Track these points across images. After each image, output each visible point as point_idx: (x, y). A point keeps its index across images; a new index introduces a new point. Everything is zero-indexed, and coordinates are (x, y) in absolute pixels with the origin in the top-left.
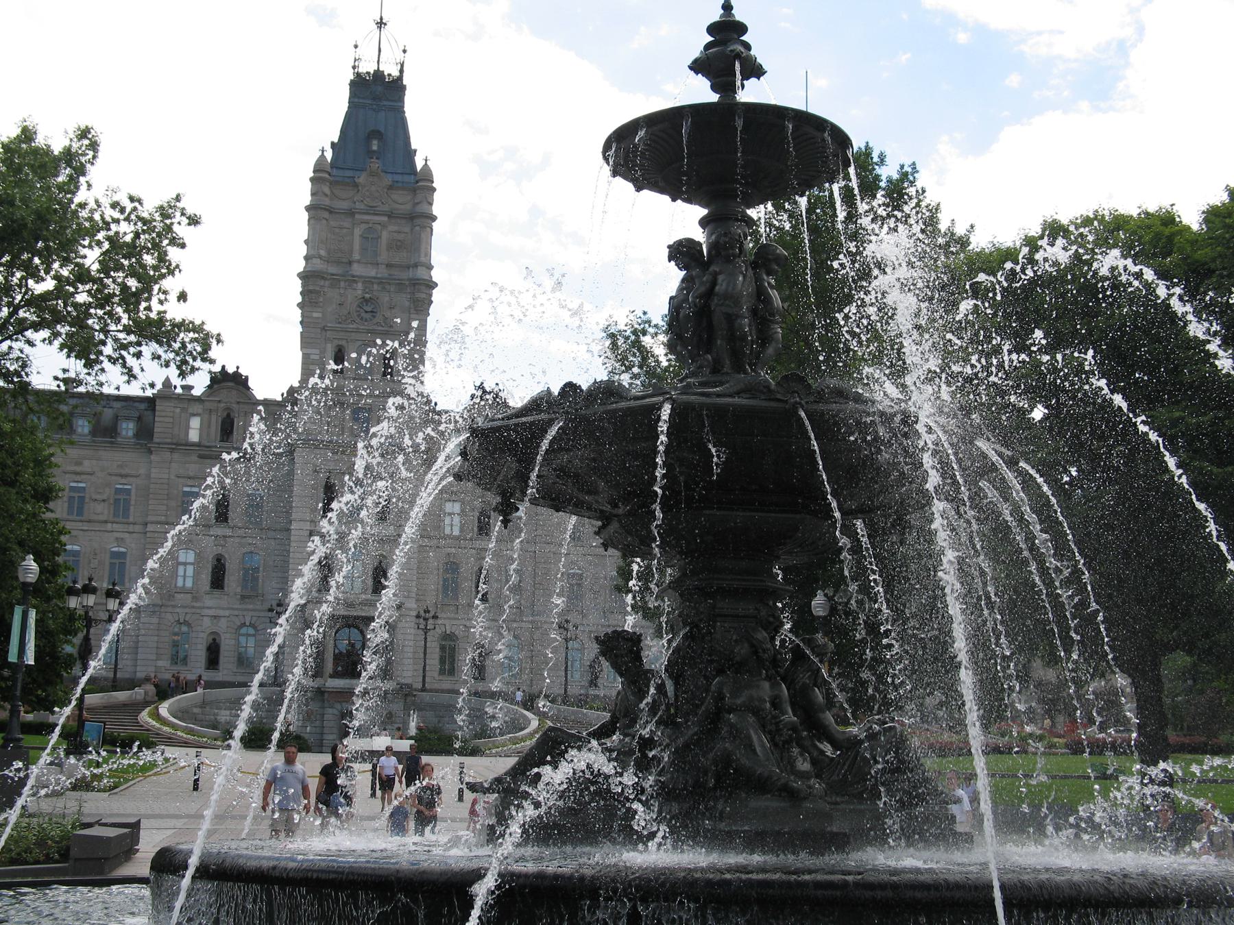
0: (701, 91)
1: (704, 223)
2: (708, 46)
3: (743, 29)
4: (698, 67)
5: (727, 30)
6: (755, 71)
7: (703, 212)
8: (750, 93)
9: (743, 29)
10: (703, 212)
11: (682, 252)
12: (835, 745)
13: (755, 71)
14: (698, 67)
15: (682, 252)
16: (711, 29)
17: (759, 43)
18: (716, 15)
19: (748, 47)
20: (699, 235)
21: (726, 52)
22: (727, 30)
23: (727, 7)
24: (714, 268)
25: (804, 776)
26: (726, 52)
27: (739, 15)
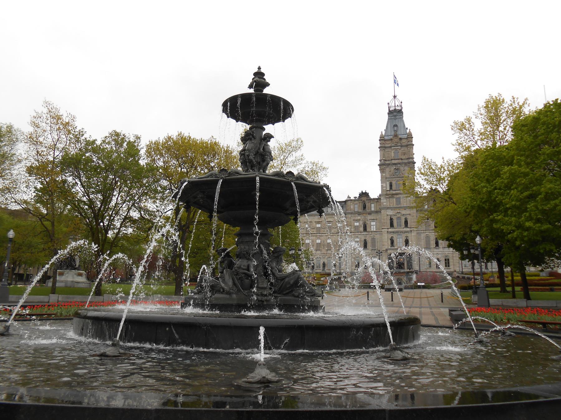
5: (259, 75)
6: (267, 85)
9: (263, 74)
16: (255, 74)
19: (265, 79)
21: (259, 81)
22: (259, 75)
23: (259, 68)
27: (262, 70)
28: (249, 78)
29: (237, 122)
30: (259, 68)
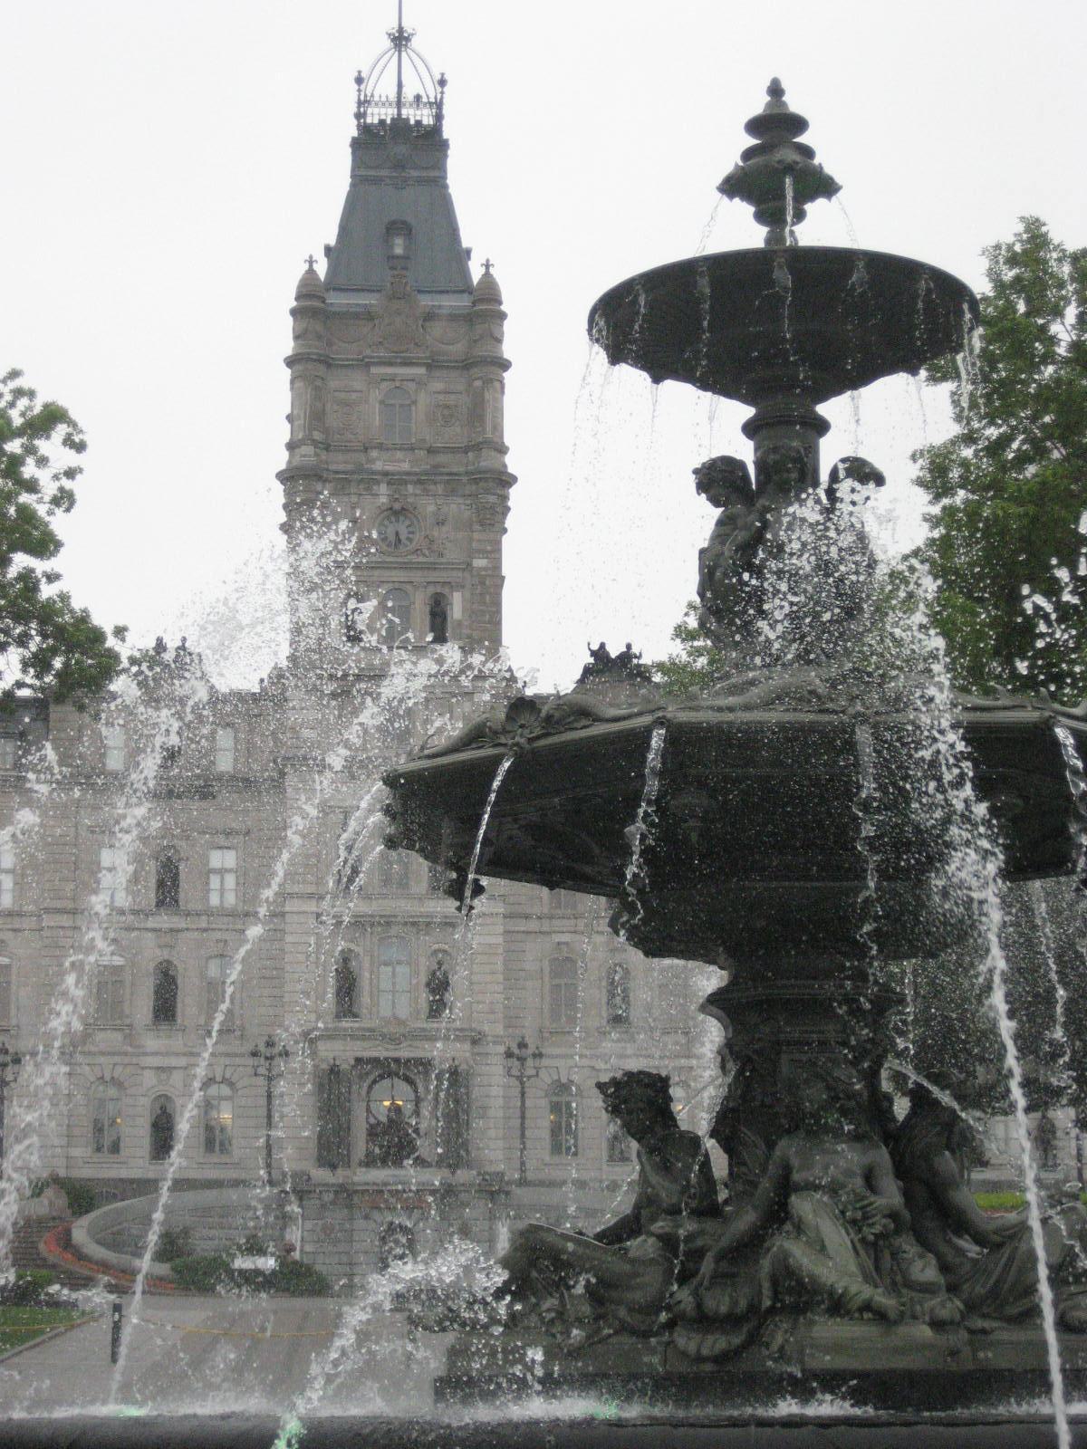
0: (740, 229)
1: (750, 429)
2: (748, 154)
3: (799, 124)
4: (733, 186)
6: (823, 186)
7: (748, 412)
8: (820, 227)
9: (799, 124)
10: (748, 412)
11: (718, 479)
12: (980, 1239)
13: (823, 186)
14: (733, 186)
15: (718, 479)
16: (754, 126)
17: (826, 144)
18: (758, 104)
19: (808, 152)
20: (745, 451)
21: (778, 165)
23: (776, 90)
24: (762, 502)
25: (928, 1289)
26: (778, 165)
27: (795, 103)
28: (732, 147)
29: (657, 379)
30: (776, 90)
